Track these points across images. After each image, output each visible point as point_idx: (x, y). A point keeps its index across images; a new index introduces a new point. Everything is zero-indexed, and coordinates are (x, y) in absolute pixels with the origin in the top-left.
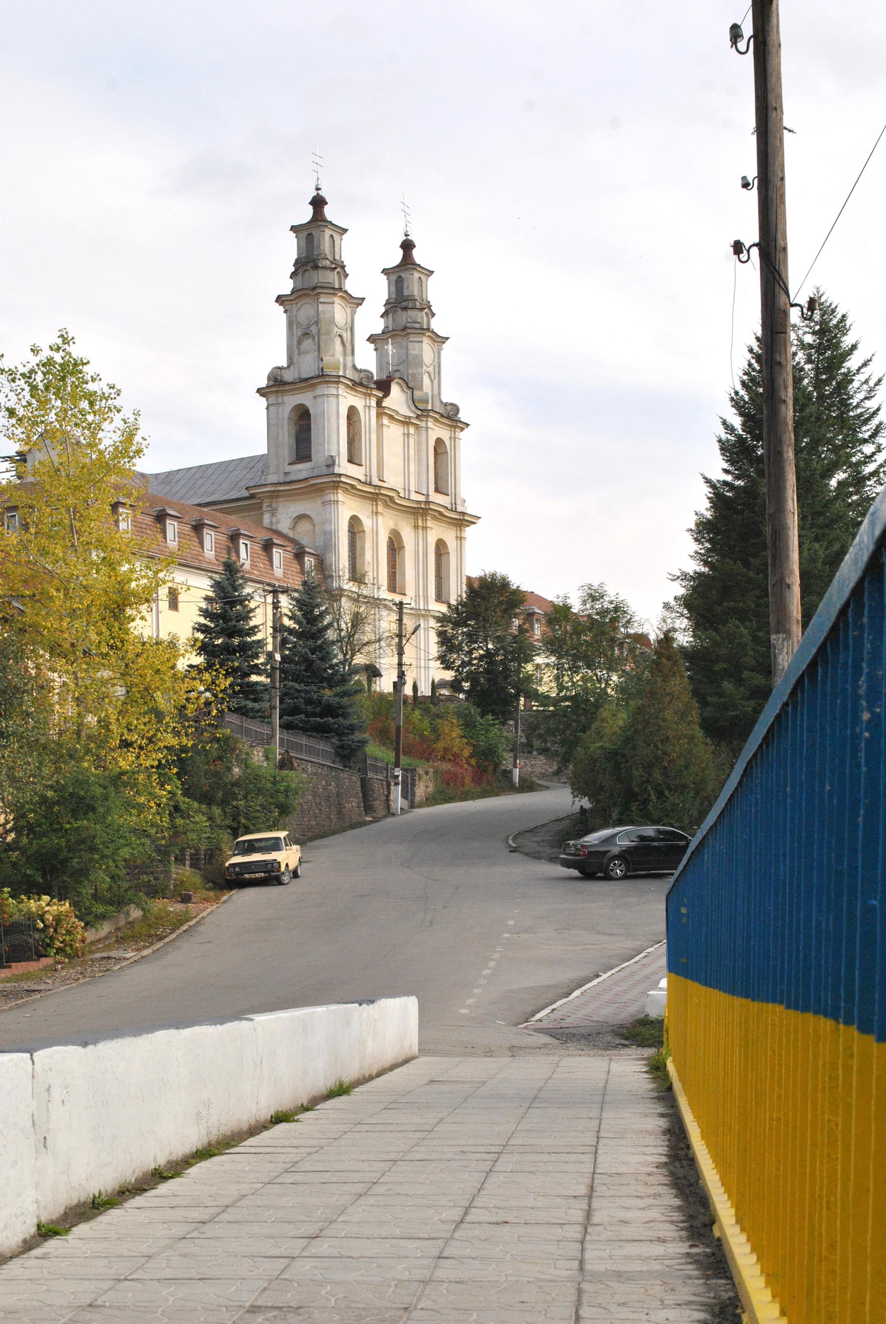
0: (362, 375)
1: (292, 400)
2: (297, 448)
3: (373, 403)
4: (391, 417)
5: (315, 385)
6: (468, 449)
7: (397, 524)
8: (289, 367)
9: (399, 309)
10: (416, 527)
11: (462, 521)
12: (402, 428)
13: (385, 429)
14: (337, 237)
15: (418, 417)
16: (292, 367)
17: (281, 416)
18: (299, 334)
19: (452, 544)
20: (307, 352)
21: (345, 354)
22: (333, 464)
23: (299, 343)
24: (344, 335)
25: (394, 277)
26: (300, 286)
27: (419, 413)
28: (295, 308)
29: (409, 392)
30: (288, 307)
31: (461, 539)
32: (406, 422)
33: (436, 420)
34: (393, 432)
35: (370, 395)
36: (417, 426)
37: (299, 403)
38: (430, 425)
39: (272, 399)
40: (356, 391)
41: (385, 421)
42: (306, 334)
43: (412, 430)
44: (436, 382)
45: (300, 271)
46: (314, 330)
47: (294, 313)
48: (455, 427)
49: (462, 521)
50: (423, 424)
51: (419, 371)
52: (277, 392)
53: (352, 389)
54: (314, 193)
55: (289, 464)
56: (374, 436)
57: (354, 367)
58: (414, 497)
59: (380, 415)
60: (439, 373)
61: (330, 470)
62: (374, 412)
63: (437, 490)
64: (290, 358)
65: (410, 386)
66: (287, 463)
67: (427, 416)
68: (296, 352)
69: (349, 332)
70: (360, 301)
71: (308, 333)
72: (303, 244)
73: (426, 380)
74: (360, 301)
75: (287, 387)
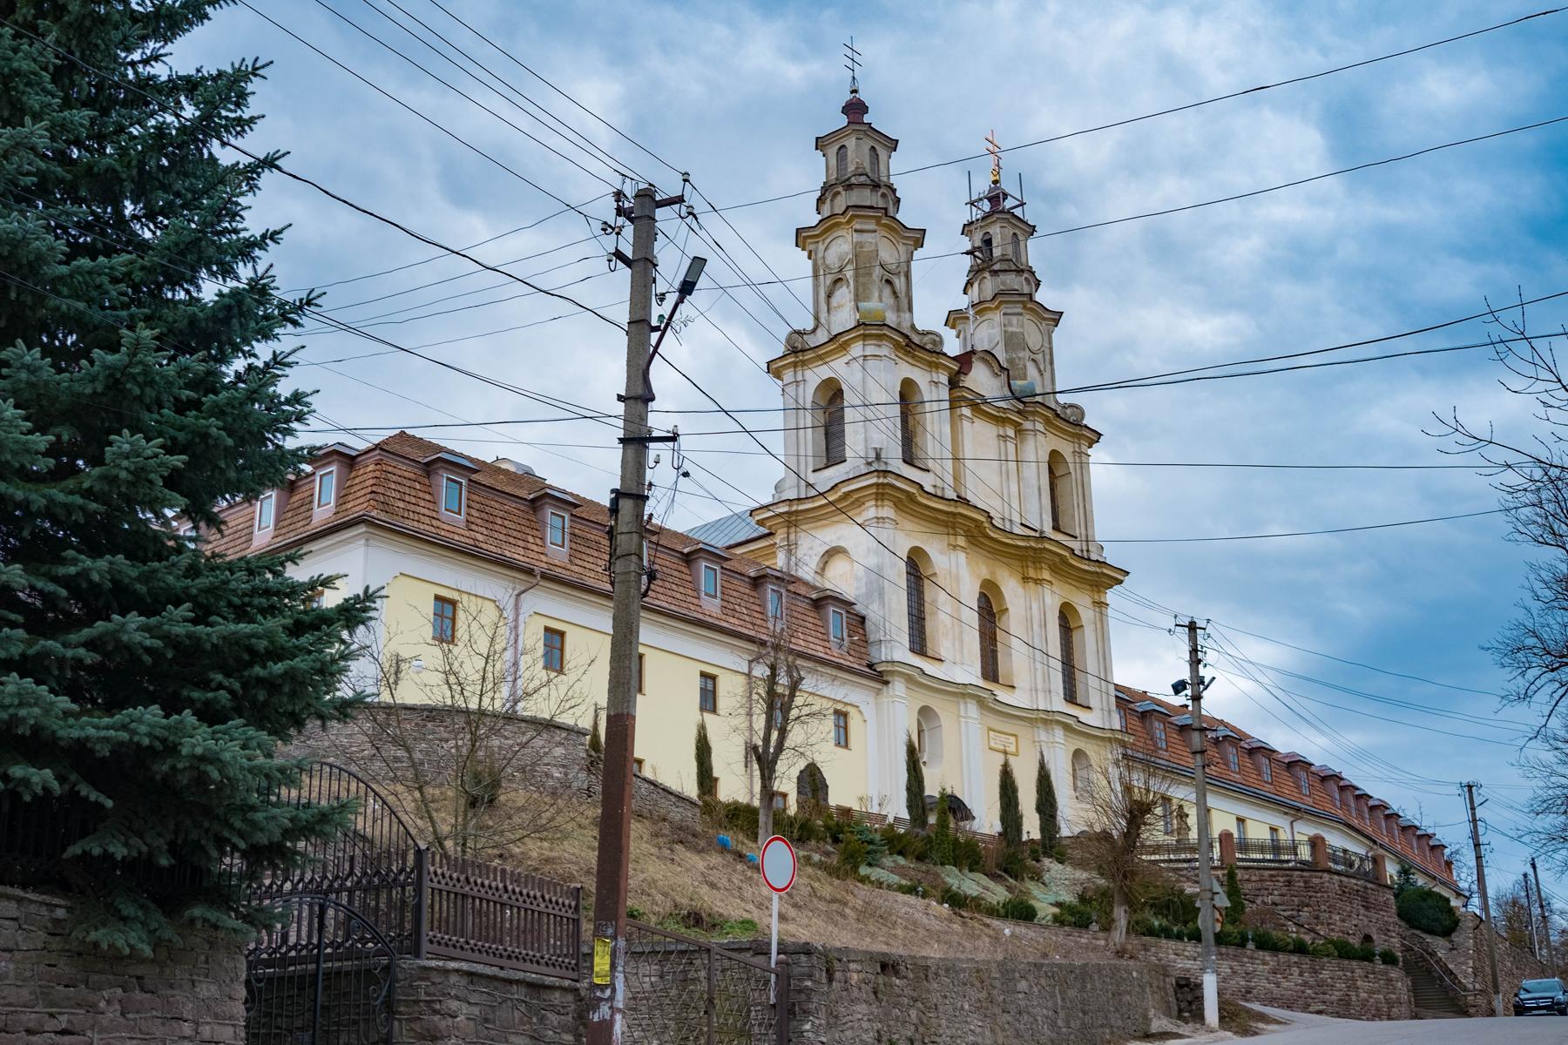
0: (926, 339)
1: (816, 375)
3: (944, 378)
4: (974, 406)
5: (844, 347)
6: (1103, 471)
7: (993, 573)
8: (814, 331)
9: (987, 275)
10: (1025, 579)
11: (1102, 578)
12: (994, 428)
13: (966, 424)
14: (882, 153)
15: (1019, 412)
16: (819, 331)
19: (1086, 614)
20: (840, 306)
21: (898, 310)
22: (878, 457)
24: (896, 281)
26: (826, 213)
27: (1021, 406)
28: (821, 247)
29: (1004, 377)
30: (811, 247)
31: (1101, 605)
33: (1048, 422)
34: (979, 436)
35: (935, 366)
36: (1019, 431)
38: (1040, 427)
39: (788, 375)
40: (914, 357)
41: (966, 411)
43: (1011, 432)
44: (1047, 375)
45: (829, 195)
46: (849, 274)
47: (820, 255)
48: (1080, 437)
49: (1102, 578)
50: (1028, 425)
52: (795, 365)
53: (907, 353)
54: (849, 97)
56: (947, 429)
57: (913, 327)
58: (1018, 530)
59: (954, 403)
60: (1052, 363)
61: (875, 466)
62: (944, 393)
63: (1056, 528)
64: (817, 318)
65: (1003, 371)
67: (1034, 413)
68: (823, 306)
69: (903, 279)
70: (917, 238)
72: (833, 162)
73: (1032, 371)
74: (917, 238)
75: (809, 355)
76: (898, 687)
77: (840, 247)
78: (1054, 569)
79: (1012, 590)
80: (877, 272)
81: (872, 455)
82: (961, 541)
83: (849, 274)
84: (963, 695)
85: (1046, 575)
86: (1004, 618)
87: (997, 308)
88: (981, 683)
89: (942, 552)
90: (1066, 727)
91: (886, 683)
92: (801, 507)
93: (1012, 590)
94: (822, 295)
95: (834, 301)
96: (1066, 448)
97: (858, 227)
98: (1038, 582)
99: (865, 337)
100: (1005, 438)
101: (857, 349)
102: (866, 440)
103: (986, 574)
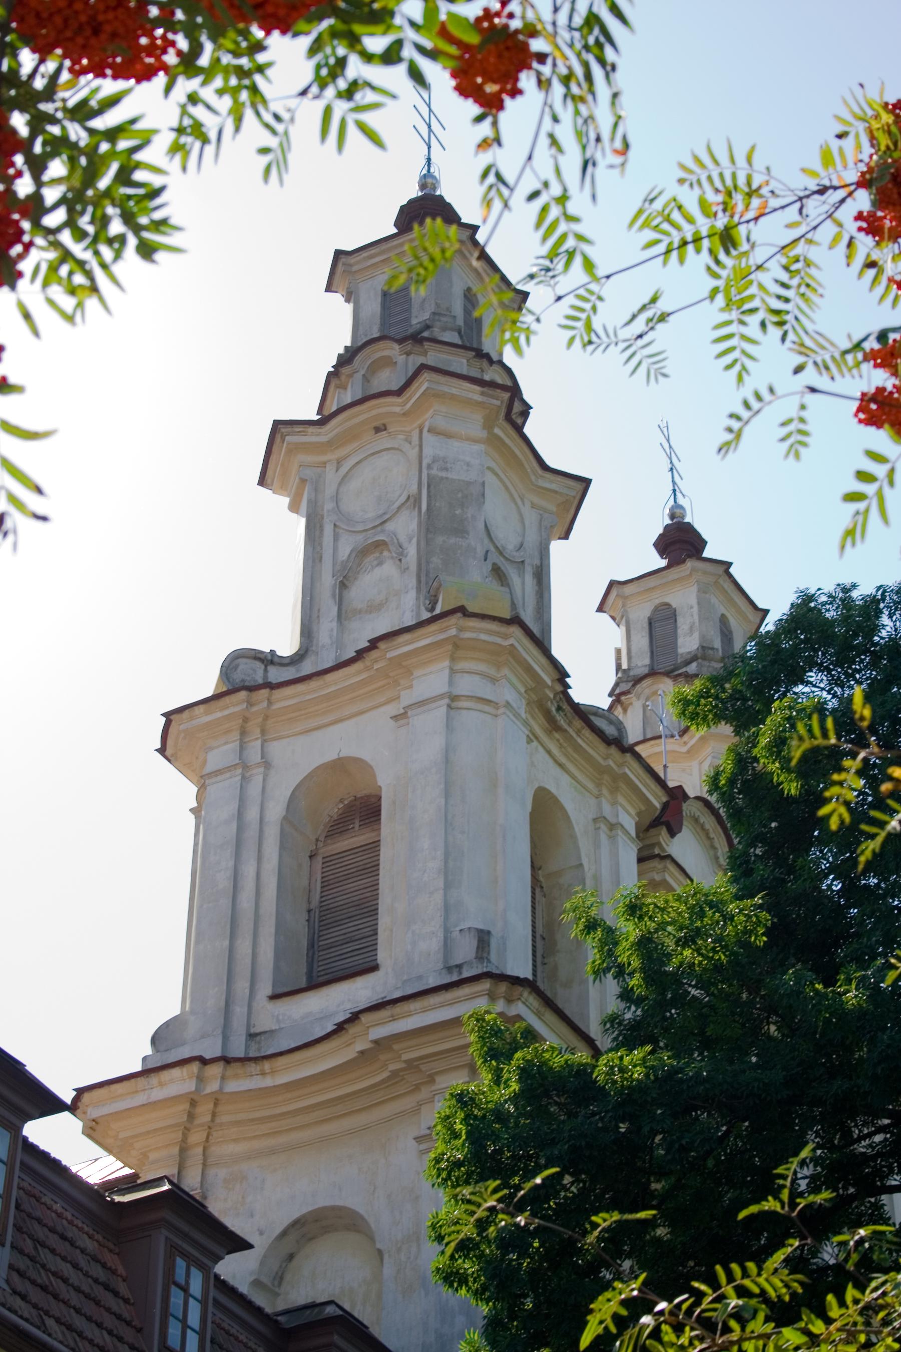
2: (311, 945)
5: (404, 668)
17: (252, 814)
18: (345, 550)
23: (343, 585)
25: (641, 612)
37: (331, 756)
42: (373, 549)
47: (330, 490)
54: (414, 192)
55: (274, 997)
62: (628, 854)
66: (265, 988)
69: (529, 579)
71: (379, 545)
77: (380, 478)
80: (476, 541)
81: (465, 950)
83: (406, 527)
92: (233, 1086)
94: (327, 580)
95: (358, 594)
97: (441, 423)
99: (457, 648)
101: (432, 680)
102: (447, 908)
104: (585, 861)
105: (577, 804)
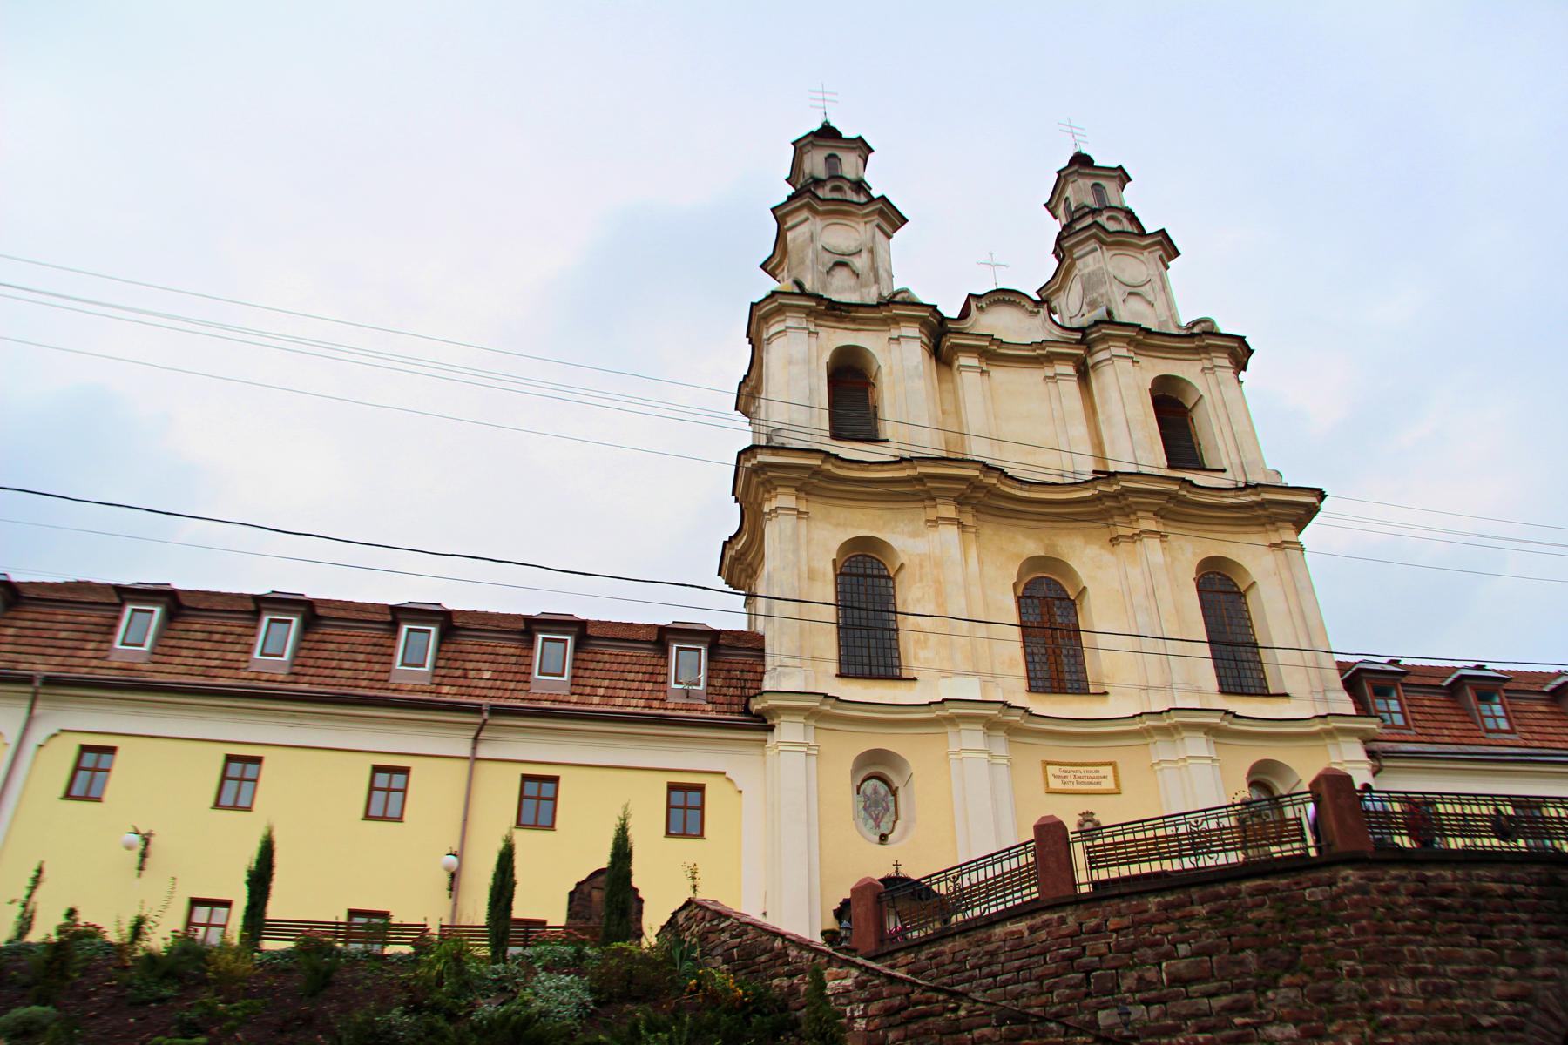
4: (983, 353)
10: (1114, 541)
15: (1079, 342)
27: (1078, 336)
29: (1044, 311)
32: (1038, 357)
33: (1131, 342)
40: (854, 320)
51: (1103, 290)
53: (840, 319)
67: (1105, 338)
69: (865, 255)
76: (788, 730)
78: (1161, 514)
79: (1091, 562)
82: (948, 510)
84: (952, 720)
85: (1150, 524)
86: (1085, 603)
87: (1074, 261)
88: (1020, 698)
89: (914, 535)
90: (1210, 730)
91: (771, 729)
93: (1091, 562)
96: (1186, 370)
98: (1133, 538)
100: (1053, 378)
103: (1031, 547)
104: (881, 363)
105: (869, 340)
